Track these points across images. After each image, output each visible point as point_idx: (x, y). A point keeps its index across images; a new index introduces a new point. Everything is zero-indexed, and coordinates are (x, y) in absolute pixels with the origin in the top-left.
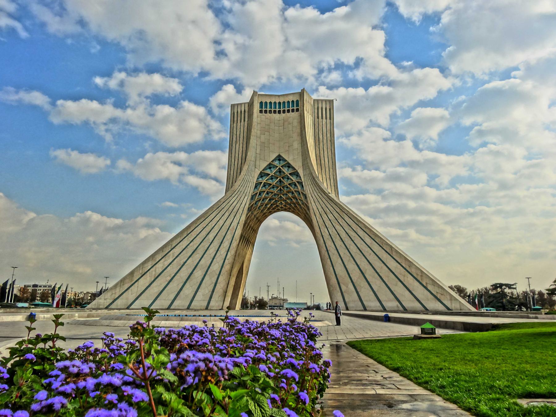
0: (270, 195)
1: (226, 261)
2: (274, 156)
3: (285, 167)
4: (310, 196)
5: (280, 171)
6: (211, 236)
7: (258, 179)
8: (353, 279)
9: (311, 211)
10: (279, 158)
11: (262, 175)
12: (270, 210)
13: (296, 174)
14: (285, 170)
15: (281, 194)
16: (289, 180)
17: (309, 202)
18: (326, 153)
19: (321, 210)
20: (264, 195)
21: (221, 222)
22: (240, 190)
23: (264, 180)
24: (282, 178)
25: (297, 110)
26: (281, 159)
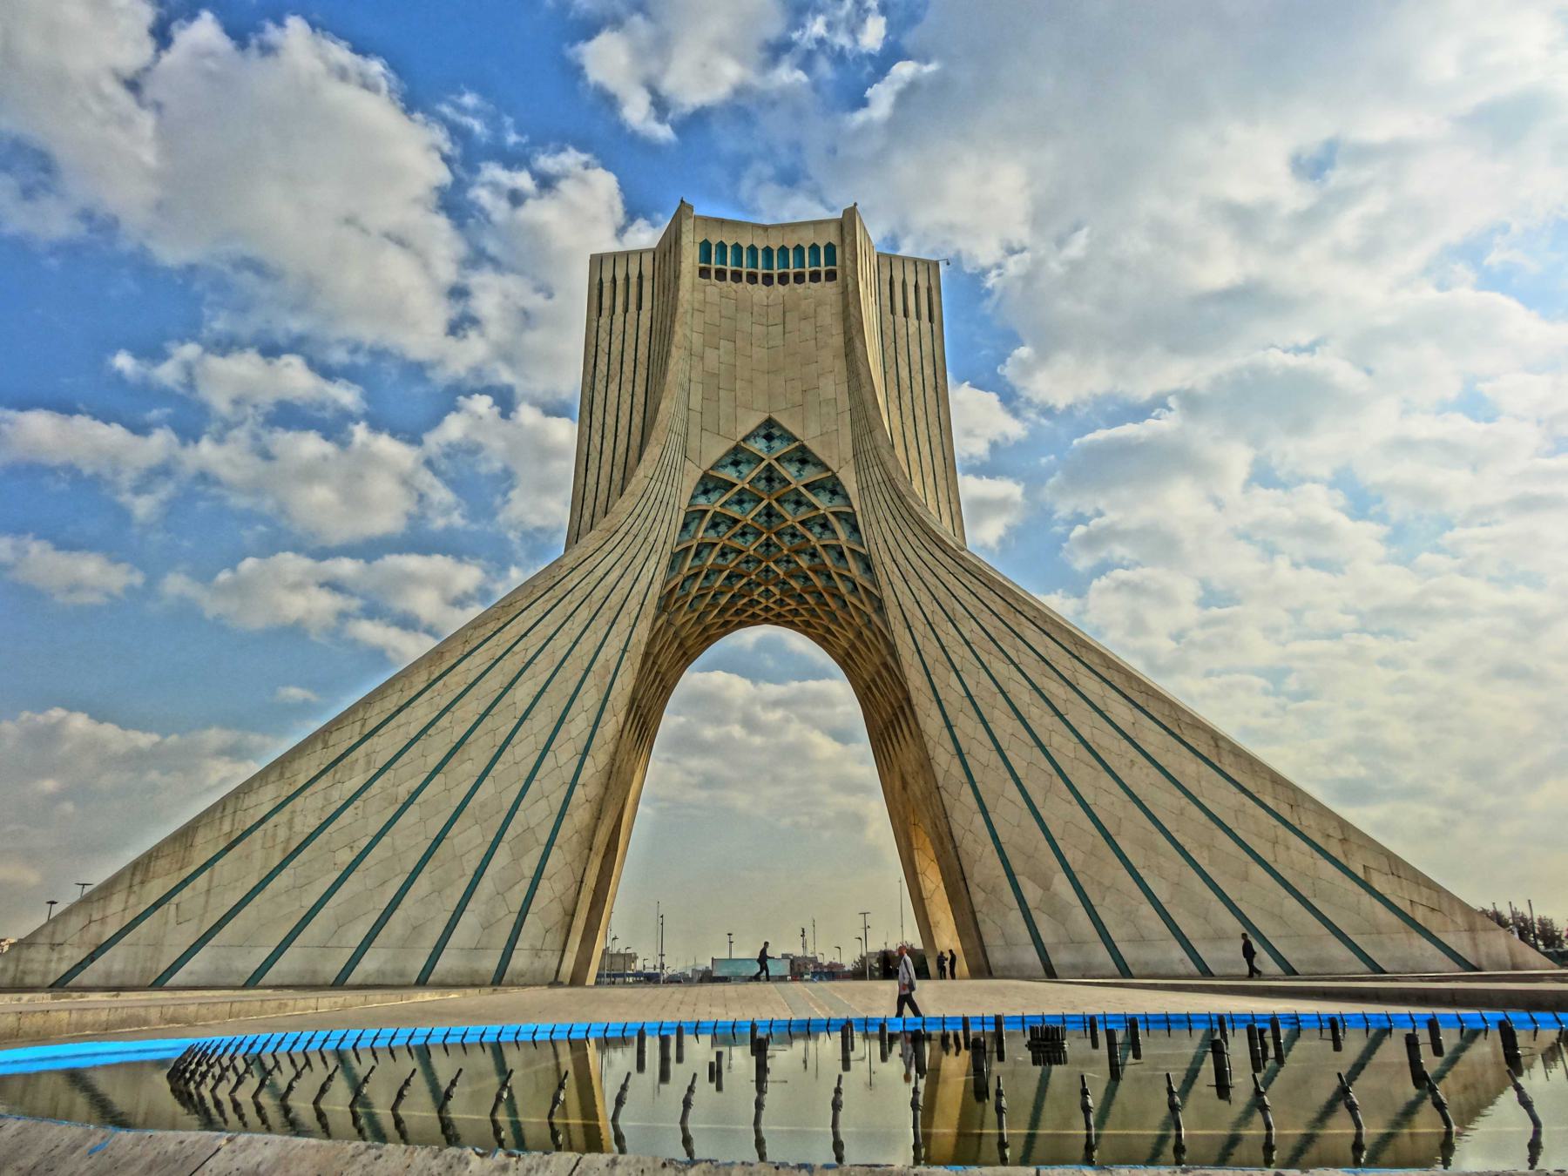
0: (732, 561)
1: (578, 790)
2: (753, 421)
3: (790, 461)
4: (887, 560)
5: (770, 476)
6: (522, 694)
7: (693, 497)
8: (1069, 858)
9: (893, 613)
10: (769, 430)
11: (709, 484)
12: (727, 616)
13: (834, 488)
14: (789, 471)
15: (768, 558)
16: (803, 509)
17: (883, 581)
18: (922, 426)
19: (930, 607)
20: (711, 559)
21: (562, 643)
22: (634, 531)
23: (714, 503)
24: (777, 500)
25: (831, 276)
26: (776, 432)
